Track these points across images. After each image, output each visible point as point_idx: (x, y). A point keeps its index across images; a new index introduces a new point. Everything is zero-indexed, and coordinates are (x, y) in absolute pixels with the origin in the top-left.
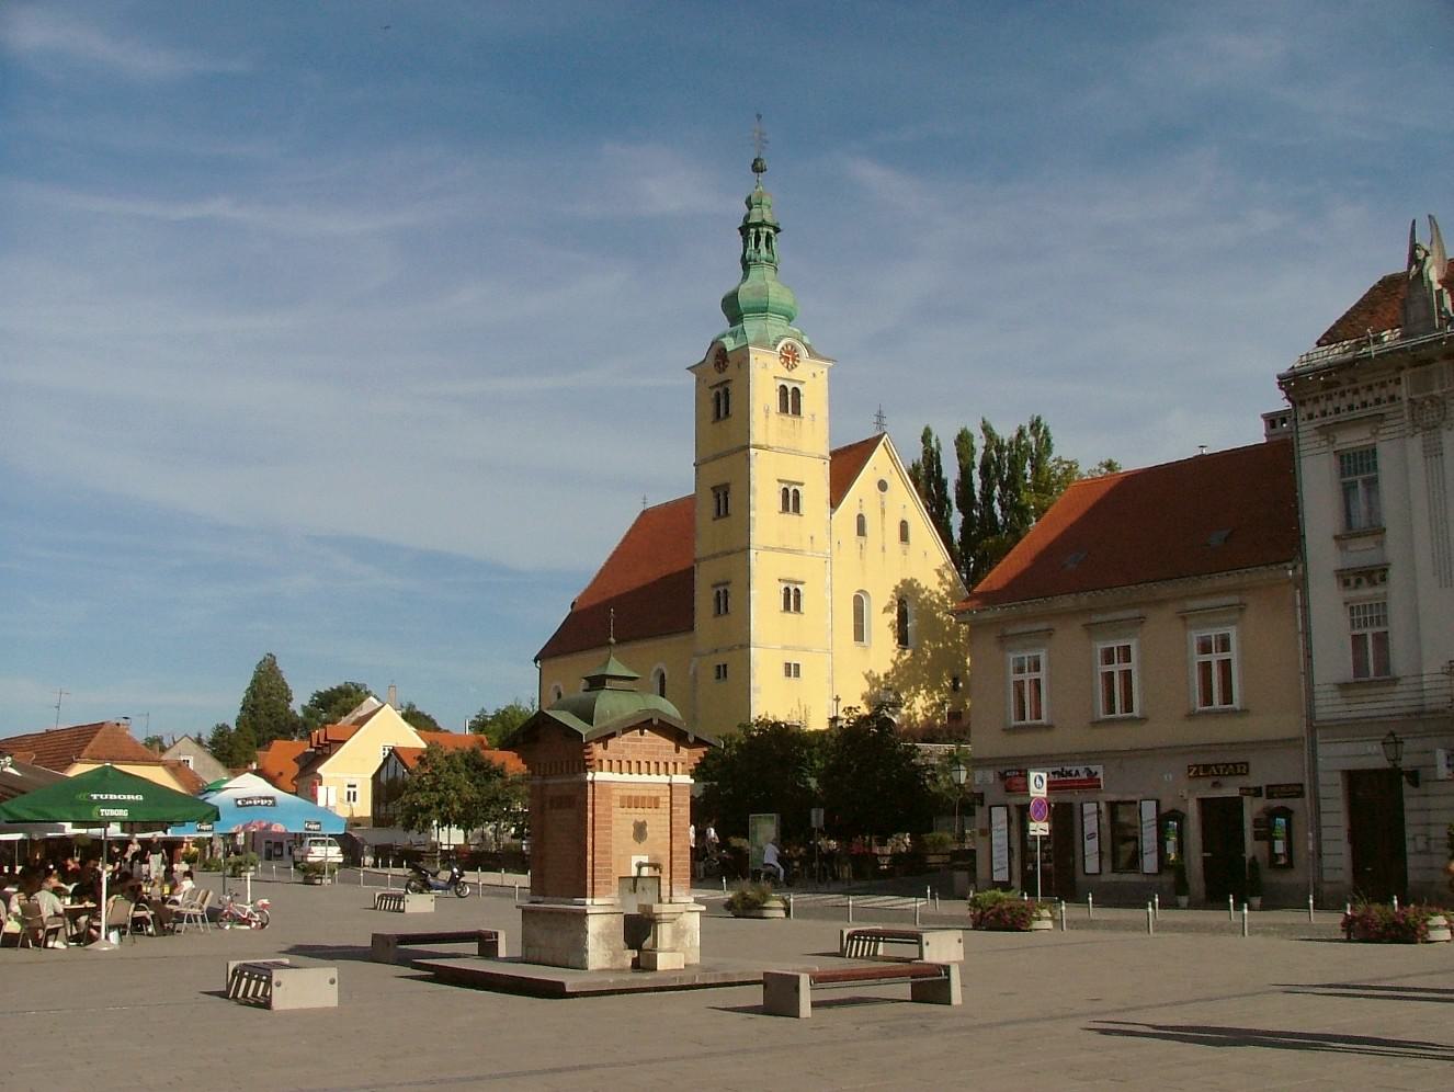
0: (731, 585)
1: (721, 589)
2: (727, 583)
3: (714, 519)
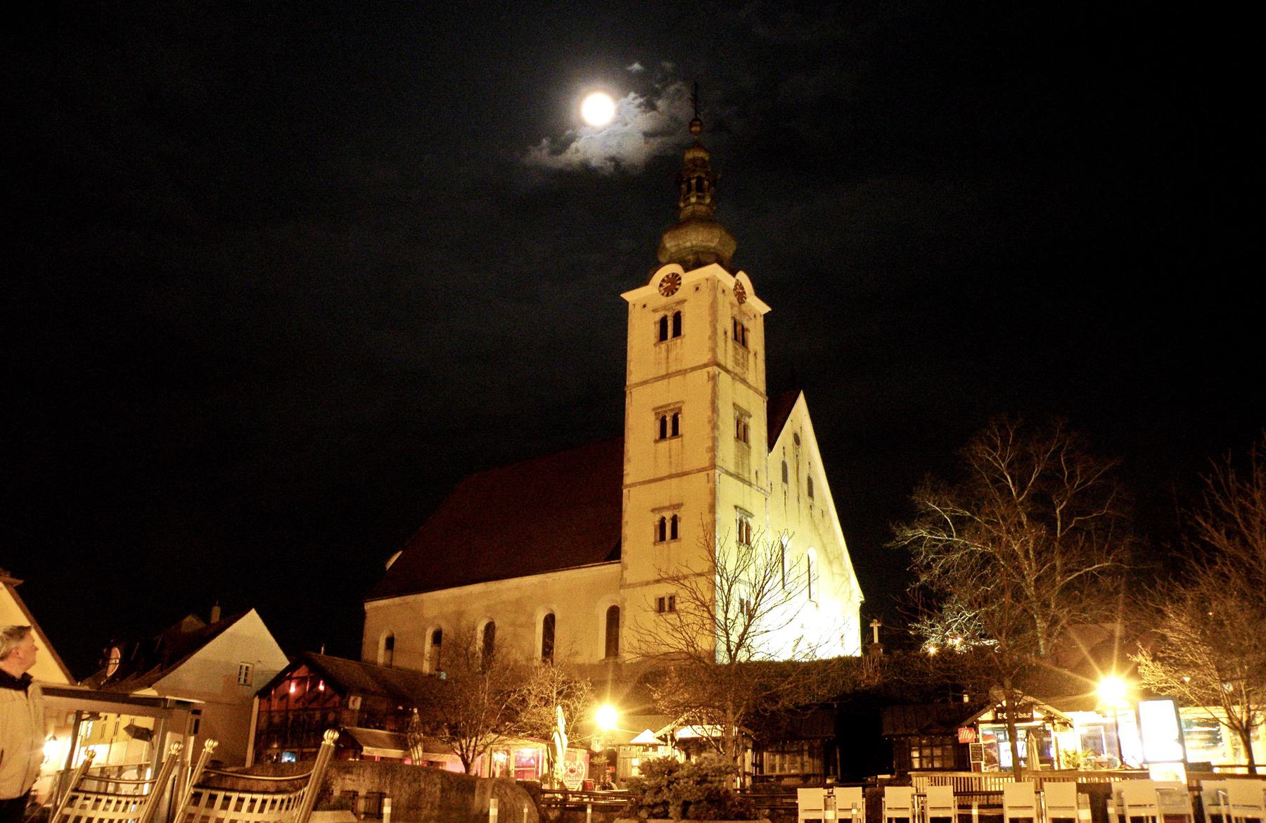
0: (683, 509)
1: (668, 515)
2: (679, 506)
3: (656, 441)
